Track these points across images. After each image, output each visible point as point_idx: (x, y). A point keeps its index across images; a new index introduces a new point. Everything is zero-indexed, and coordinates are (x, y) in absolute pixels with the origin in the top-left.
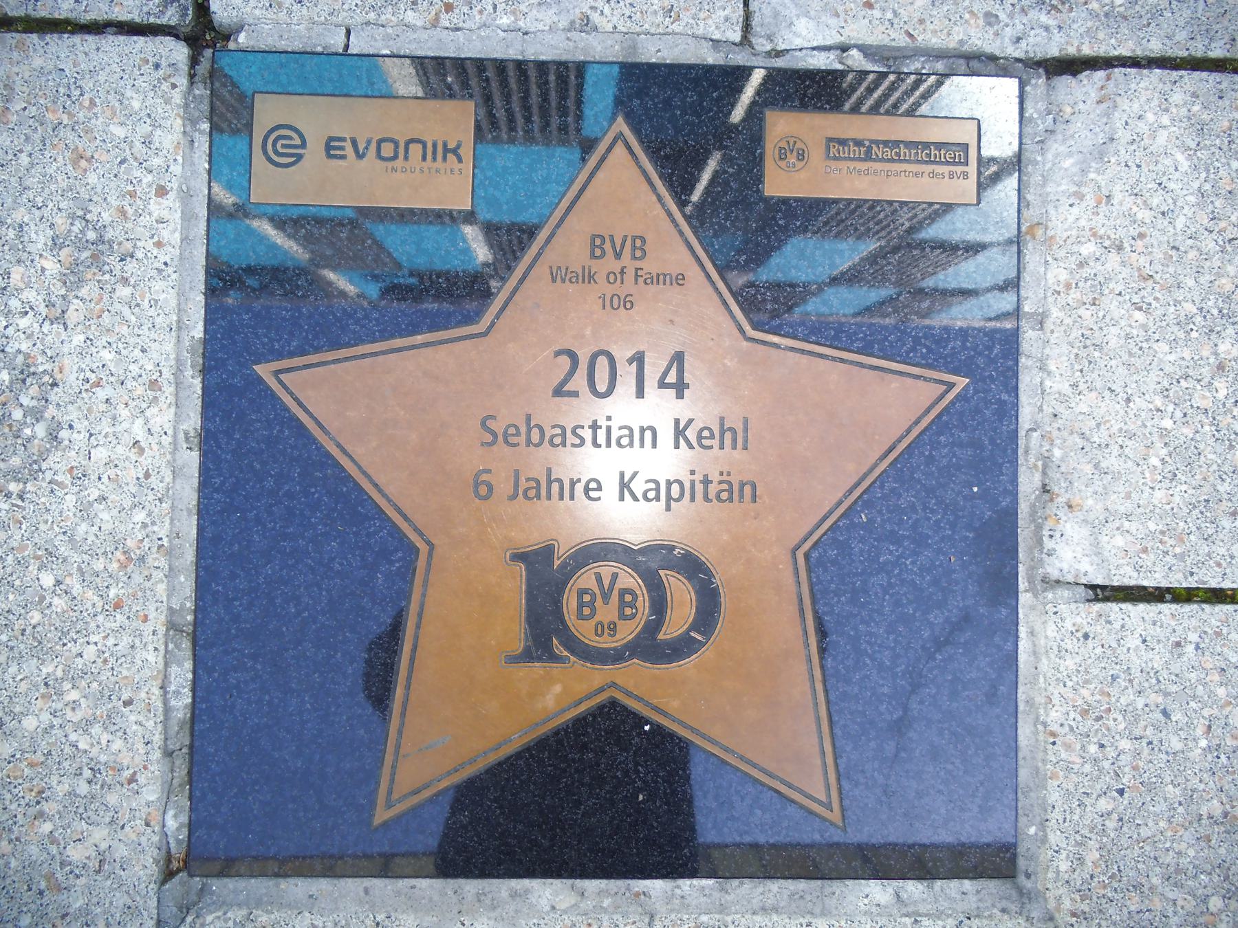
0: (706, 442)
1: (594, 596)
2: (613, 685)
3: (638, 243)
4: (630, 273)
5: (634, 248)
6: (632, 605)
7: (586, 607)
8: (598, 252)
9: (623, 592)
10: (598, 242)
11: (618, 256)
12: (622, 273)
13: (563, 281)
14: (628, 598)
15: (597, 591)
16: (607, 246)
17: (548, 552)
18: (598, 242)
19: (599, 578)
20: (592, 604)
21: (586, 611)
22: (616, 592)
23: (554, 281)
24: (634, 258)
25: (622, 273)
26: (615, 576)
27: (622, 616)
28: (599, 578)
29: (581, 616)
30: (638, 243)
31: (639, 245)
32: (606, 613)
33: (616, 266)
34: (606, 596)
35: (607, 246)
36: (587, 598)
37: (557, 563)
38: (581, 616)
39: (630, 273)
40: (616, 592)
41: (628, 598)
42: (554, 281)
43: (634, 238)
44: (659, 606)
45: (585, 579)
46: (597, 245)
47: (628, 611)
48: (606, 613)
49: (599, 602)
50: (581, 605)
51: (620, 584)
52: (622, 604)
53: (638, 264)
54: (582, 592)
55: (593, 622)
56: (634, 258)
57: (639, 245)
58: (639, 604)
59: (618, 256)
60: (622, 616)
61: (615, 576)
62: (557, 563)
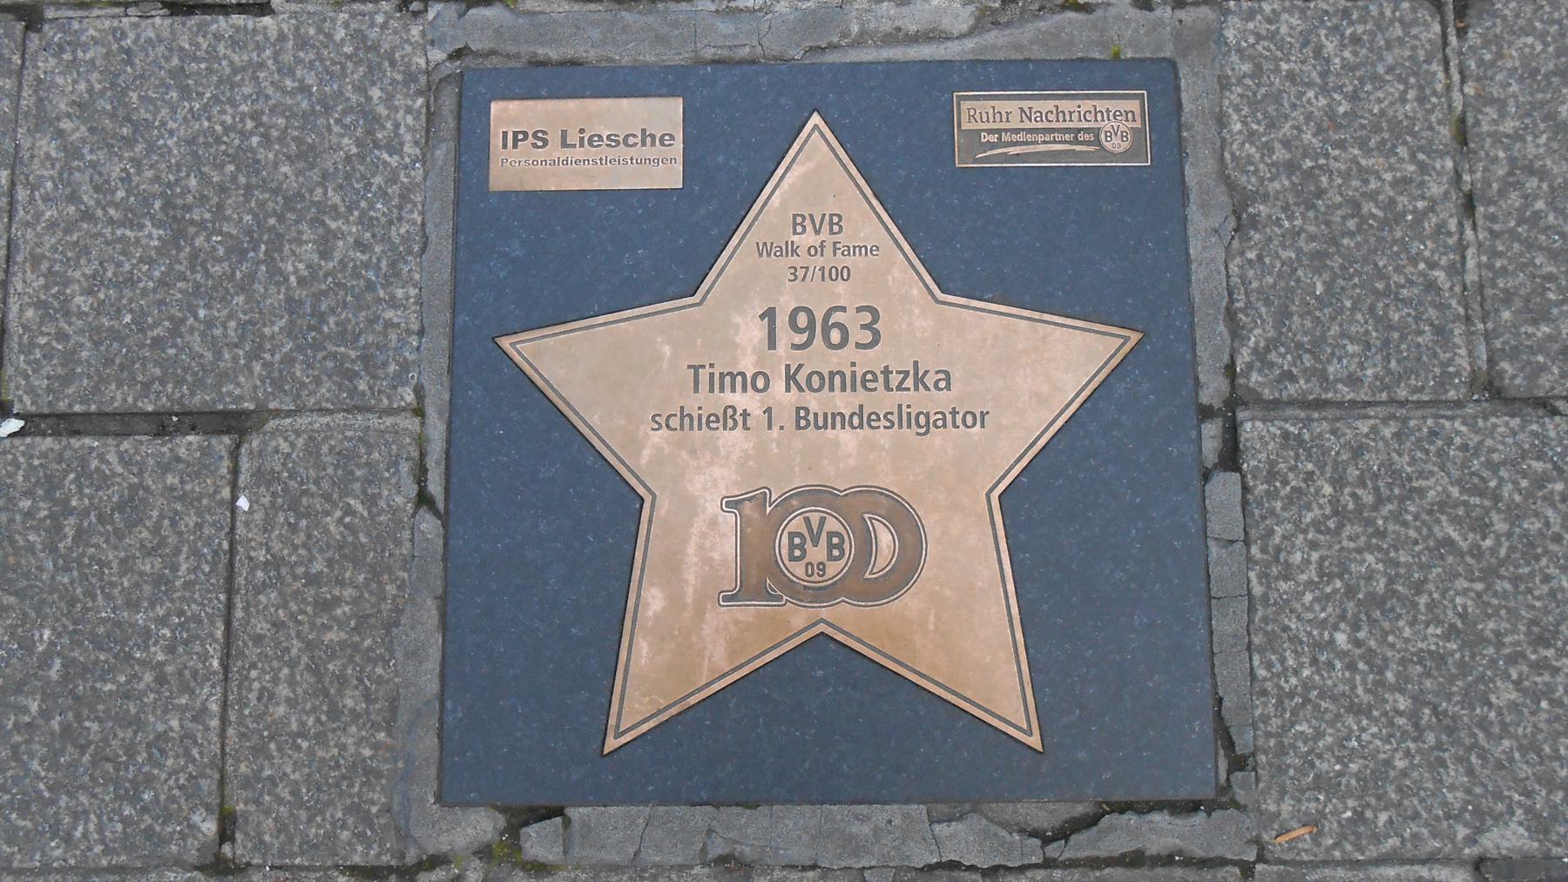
2: (822, 621)
3: (836, 220)
4: (828, 250)
5: (831, 223)
6: (840, 547)
7: (798, 549)
8: (799, 229)
9: (831, 535)
10: (799, 220)
11: (817, 232)
12: (822, 246)
13: (769, 255)
16: (808, 222)
17: (761, 499)
18: (799, 220)
19: (807, 520)
20: (802, 547)
22: (824, 536)
23: (761, 255)
24: (832, 232)
25: (822, 246)
26: (822, 521)
27: (831, 558)
28: (807, 520)
29: (792, 558)
30: (836, 220)
31: (835, 222)
32: (817, 553)
34: (815, 544)
35: (808, 222)
36: (797, 541)
37: (769, 509)
39: (828, 250)
40: (824, 536)
41: (835, 540)
42: (761, 255)
43: (831, 216)
44: (866, 545)
45: (797, 524)
47: (836, 553)
48: (817, 553)
50: (792, 547)
51: (827, 528)
52: (831, 546)
54: (792, 535)
56: (832, 232)
57: (835, 222)
58: (846, 546)
59: (817, 232)
60: (831, 558)
61: (822, 521)
62: (769, 509)
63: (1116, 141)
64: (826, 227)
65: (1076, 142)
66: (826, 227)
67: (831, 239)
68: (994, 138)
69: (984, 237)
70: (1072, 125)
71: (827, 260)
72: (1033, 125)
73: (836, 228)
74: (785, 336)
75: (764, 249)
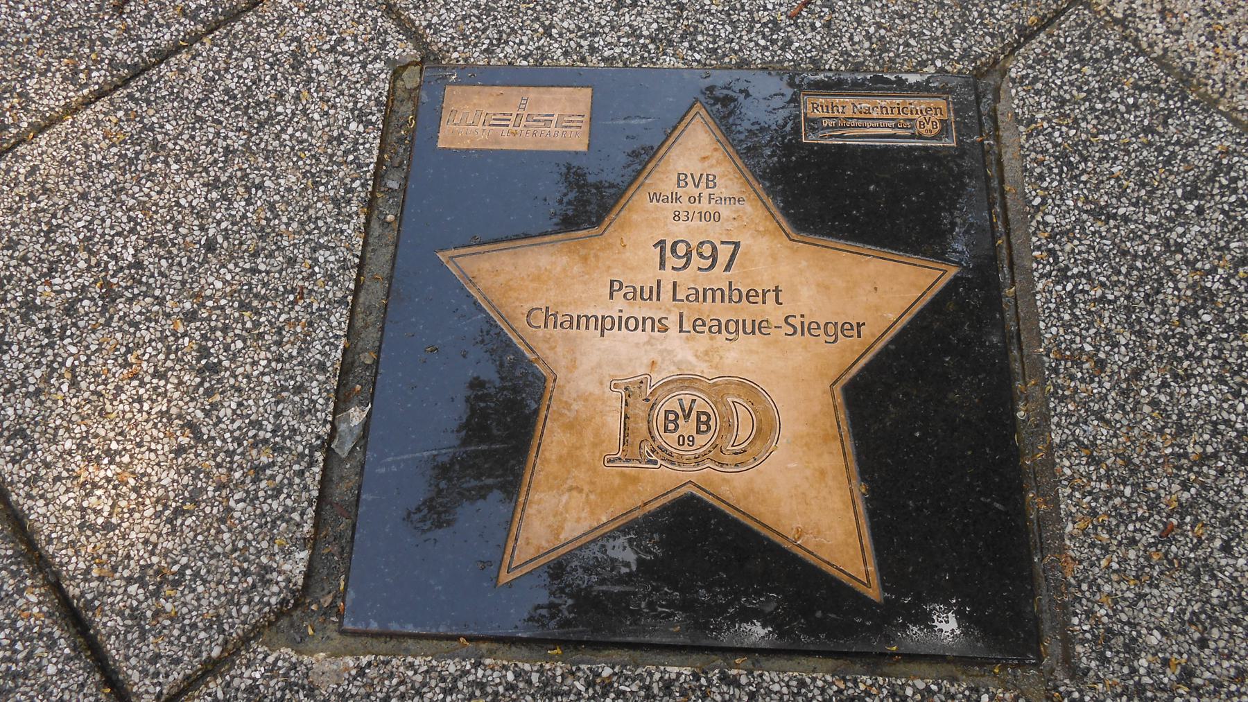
0: (756, 299)
1: (677, 416)
6: (707, 423)
8: (682, 183)
11: (696, 186)
14: (704, 418)
15: (680, 414)
16: (689, 179)
18: (682, 177)
20: (675, 421)
21: (671, 426)
26: (694, 401)
30: (711, 178)
32: (687, 428)
33: (696, 192)
34: (687, 417)
35: (689, 179)
36: (672, 417)
38: (666, 430)
39: (705, 200)
41: (704, 418)
46: (681, 180)
47: (703, 428)
48: (687, 428)
49: (681, 422)
53: (711, 191)
55: (676, 435)
56: (707, 187)
58: (712, 423)
59: (696, 186)
60: (699, 431)
61: (694, 401)
63: (929, 127)
64: (703, 185)
65: (896, 126)
66: (703, 185)
67: (706, 193)
68: (831, 123)
69: (826, 192)
70: (890, 116)
71: (705, 206)
72: (863, 116)
73: (711, 184)
74: (671, 261)
75: (655, 197)
